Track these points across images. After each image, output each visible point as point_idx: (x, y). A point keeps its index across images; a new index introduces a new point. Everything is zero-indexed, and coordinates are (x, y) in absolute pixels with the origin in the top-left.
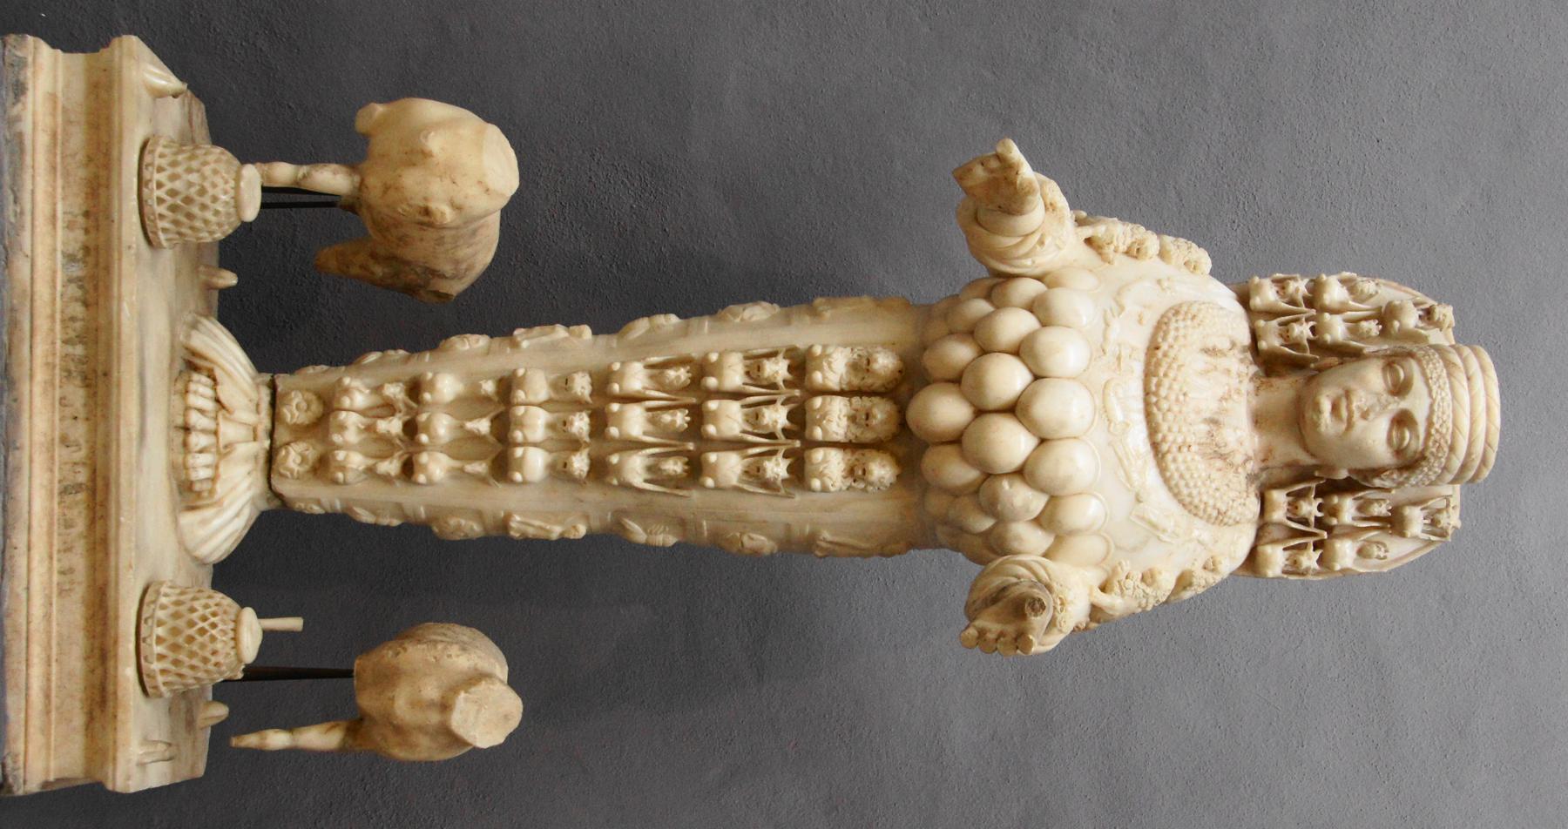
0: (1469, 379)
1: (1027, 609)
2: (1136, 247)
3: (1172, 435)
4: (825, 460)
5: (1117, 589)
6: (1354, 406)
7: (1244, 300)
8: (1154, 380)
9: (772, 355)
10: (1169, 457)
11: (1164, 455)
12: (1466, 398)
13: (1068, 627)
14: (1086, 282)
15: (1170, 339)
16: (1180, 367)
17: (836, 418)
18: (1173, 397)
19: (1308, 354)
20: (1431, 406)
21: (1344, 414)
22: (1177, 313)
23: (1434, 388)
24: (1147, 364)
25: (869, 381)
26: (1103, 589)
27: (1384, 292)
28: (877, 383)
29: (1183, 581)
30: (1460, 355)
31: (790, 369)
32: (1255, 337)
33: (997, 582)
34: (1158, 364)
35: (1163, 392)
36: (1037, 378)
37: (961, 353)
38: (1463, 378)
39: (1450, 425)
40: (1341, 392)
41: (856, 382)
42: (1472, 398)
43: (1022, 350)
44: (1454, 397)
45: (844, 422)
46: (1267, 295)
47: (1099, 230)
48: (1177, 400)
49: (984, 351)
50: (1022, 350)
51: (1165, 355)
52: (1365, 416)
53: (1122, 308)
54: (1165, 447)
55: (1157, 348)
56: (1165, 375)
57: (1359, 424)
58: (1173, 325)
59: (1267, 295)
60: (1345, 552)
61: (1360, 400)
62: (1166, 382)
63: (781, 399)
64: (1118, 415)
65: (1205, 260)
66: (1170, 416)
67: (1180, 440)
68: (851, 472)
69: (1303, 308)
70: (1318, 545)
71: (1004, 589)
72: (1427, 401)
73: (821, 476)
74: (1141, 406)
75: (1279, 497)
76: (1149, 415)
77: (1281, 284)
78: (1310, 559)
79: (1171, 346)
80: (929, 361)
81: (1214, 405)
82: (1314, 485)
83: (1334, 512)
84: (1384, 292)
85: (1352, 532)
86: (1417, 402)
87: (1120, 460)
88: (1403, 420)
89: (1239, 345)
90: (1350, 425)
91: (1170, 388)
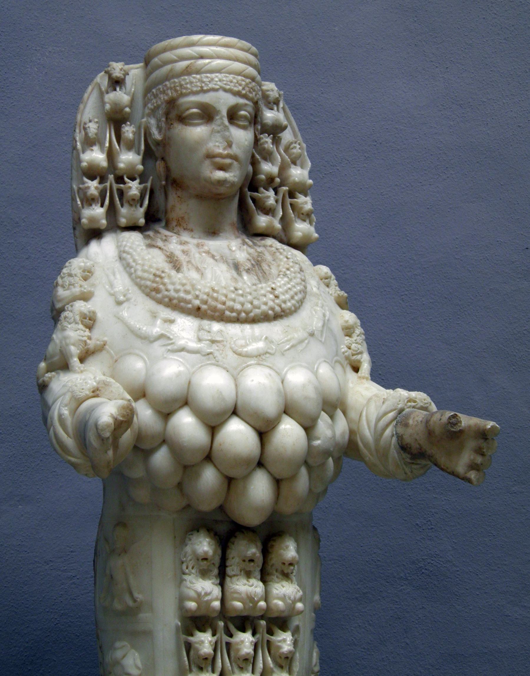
0: (202, 57)
1: (456, 429)
2: (87, 321)
3: (266, 303)
4: (283, 598)
5: (359, 357)
6: (221, 151)
7: (95, 234)
8: (227, 313)
9: (189, 647)
10: (283, 306)
11: (283, 311)
12: (217, 63)
13: (429, 399)
14: (136, 366)
15: (189, 297)
16: (213, 290)
17: (246, 588)
18: (241, 299)
19: (149, 185)
20: (225, 90)
21: (228, 161)
22: (157, 290)
23: (211, 86)
24: (213, 318)
25: (217, 560)
26: (356, 369)
27: (89, 115)
28: (219, 552)
29: (342, 305)
30: (176, 61)
31: (244, 630)
32: (132, 228)
33: (394, 453)
34: (215, 309)
35: (238, 307)
36: (235, 412)
37: (209, 477)
38: (201, 62)
39: (240, 78)
40: (207, 162)
41: (216, 571)
42: (219, 57)
43: (213, 425)
44: (219, 71)
45: (253, 581)
46: (97, 212)
47: (74, 350)
48: (242, 295)
49: (209, 457)
50: (213, 425)
51: (205, 302)
52: (230, 145)
53: (162, 336)
54: (277, 309)
55: (199, 309)
56: (224, 303)
57: (235, 150)
58: (173, 294)
59: (97, 212)
60: (298, 174)
61: (217, 146)
62: (230, 303)
63: (226, 638)
64: (260, 345)
65: (76, 264)
66: (256, 302)
67: (271, 296)
68: (286, 576)
69: (108, 184)
70: (292, 195)
71: (404, 448)
72: (221, 93)
73: (294, 602)
74: (247, 328)
75: (262, 221)
76: (254, 321)
77: (89, 201)
78: (306, 202)
79: (197, 297)
80: (207, 505)
81: (224, 267)
82: (249, 193)
83: (271, 180)
84: (89, 115)
85: (283, 168)
86: (224, 101)
87: (293, 346)
88: (233, 116)
89: (148, 242)
90: (235, 158)
91: (234, 300)
